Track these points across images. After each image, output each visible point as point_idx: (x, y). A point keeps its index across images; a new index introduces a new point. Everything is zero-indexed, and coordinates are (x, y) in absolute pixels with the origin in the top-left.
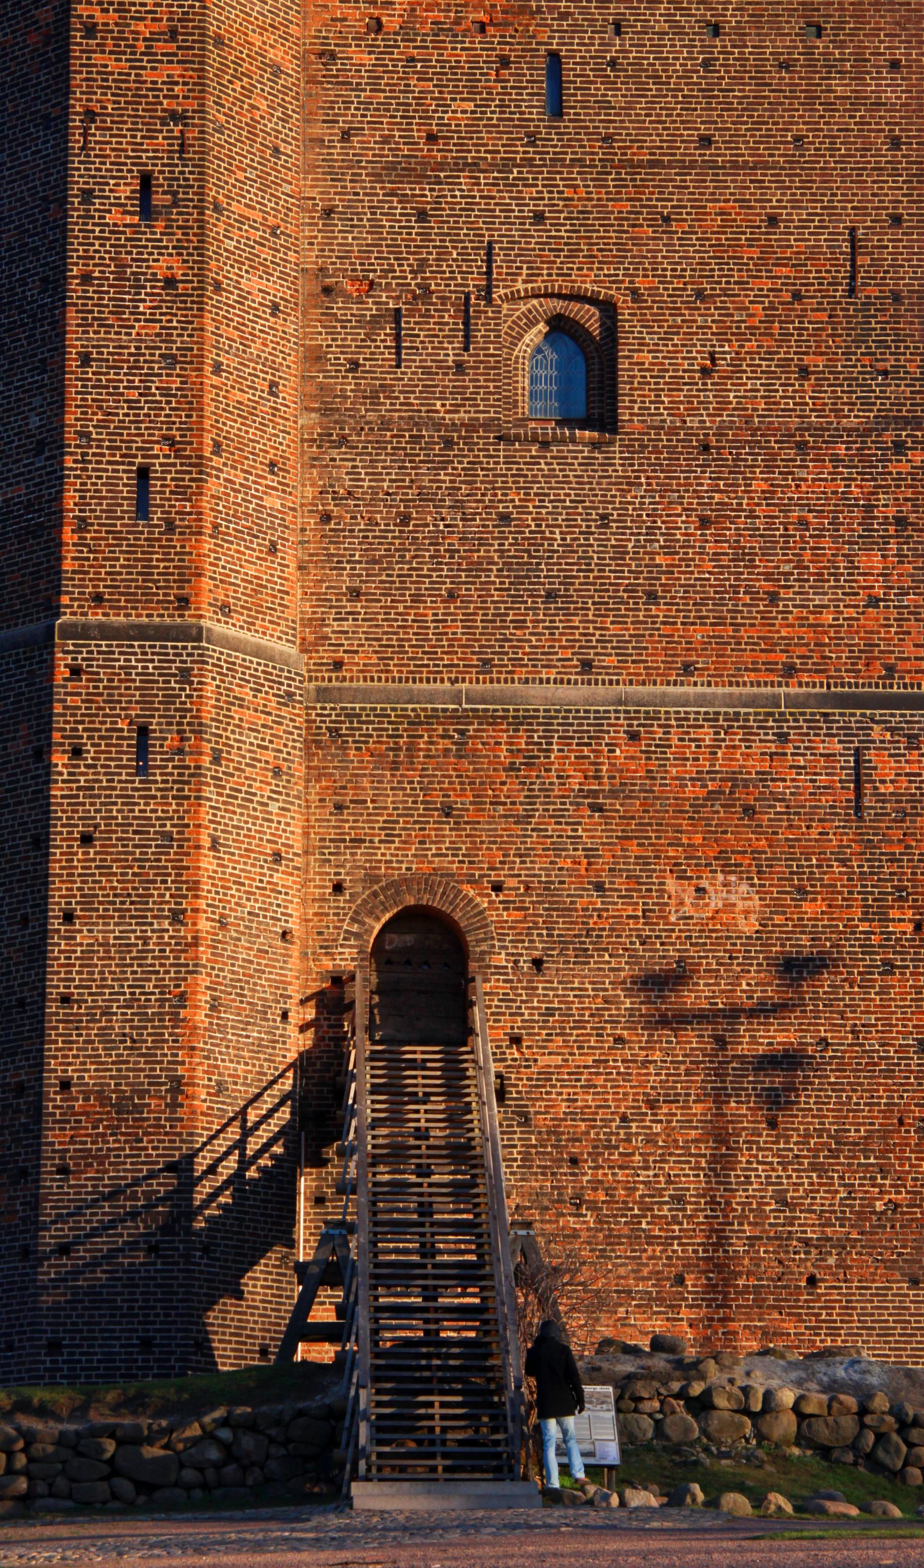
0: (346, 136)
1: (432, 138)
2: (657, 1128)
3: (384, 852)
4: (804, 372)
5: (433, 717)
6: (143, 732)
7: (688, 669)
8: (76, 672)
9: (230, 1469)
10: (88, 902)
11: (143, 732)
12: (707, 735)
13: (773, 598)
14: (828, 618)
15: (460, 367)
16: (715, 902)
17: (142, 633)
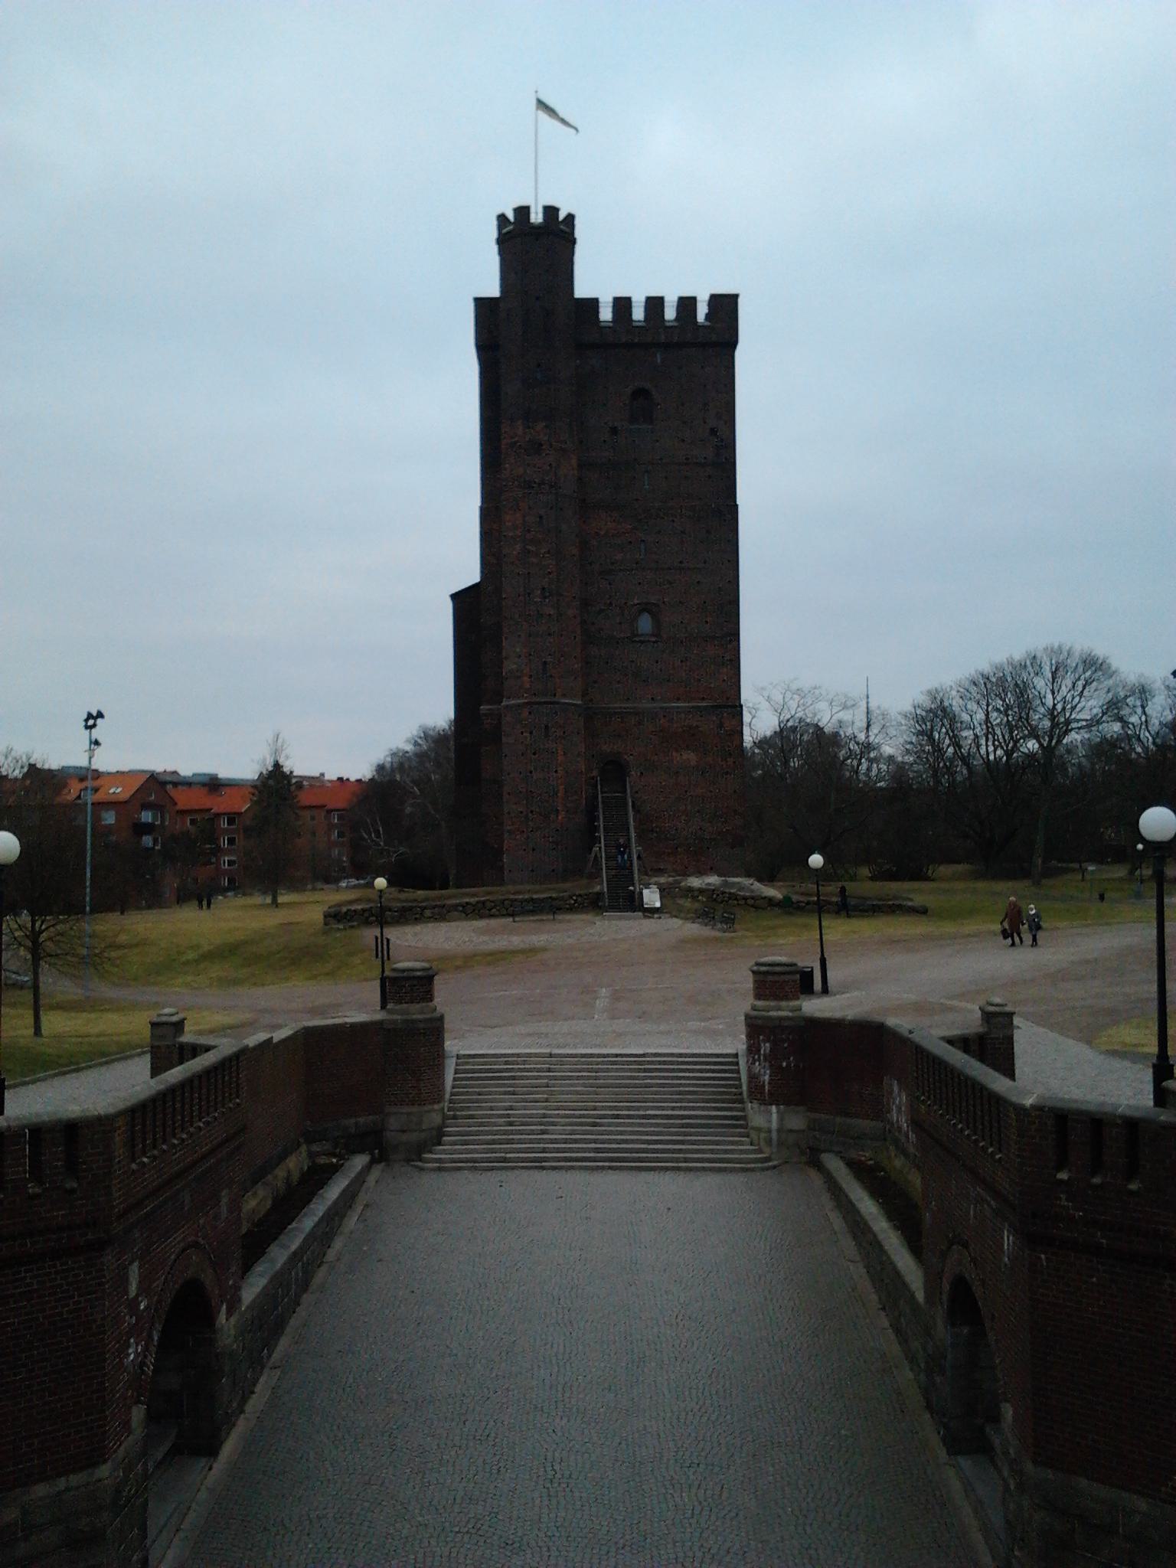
0: (591, 564)
1: (612, 564)
2: (671, 813)
3: (604, 747)
4: (707, 622)
5: (615, 713)
6: (547, 727)
7: (678, 699)
8: (530, 713)
9: (576, 905)
10: (535, 769)
11: (547, 727)
12: (683, 715)
13: (699, 680)
14: (712, 685)
15: (620, 623)
16: (685, 757)
17: (545, 703)
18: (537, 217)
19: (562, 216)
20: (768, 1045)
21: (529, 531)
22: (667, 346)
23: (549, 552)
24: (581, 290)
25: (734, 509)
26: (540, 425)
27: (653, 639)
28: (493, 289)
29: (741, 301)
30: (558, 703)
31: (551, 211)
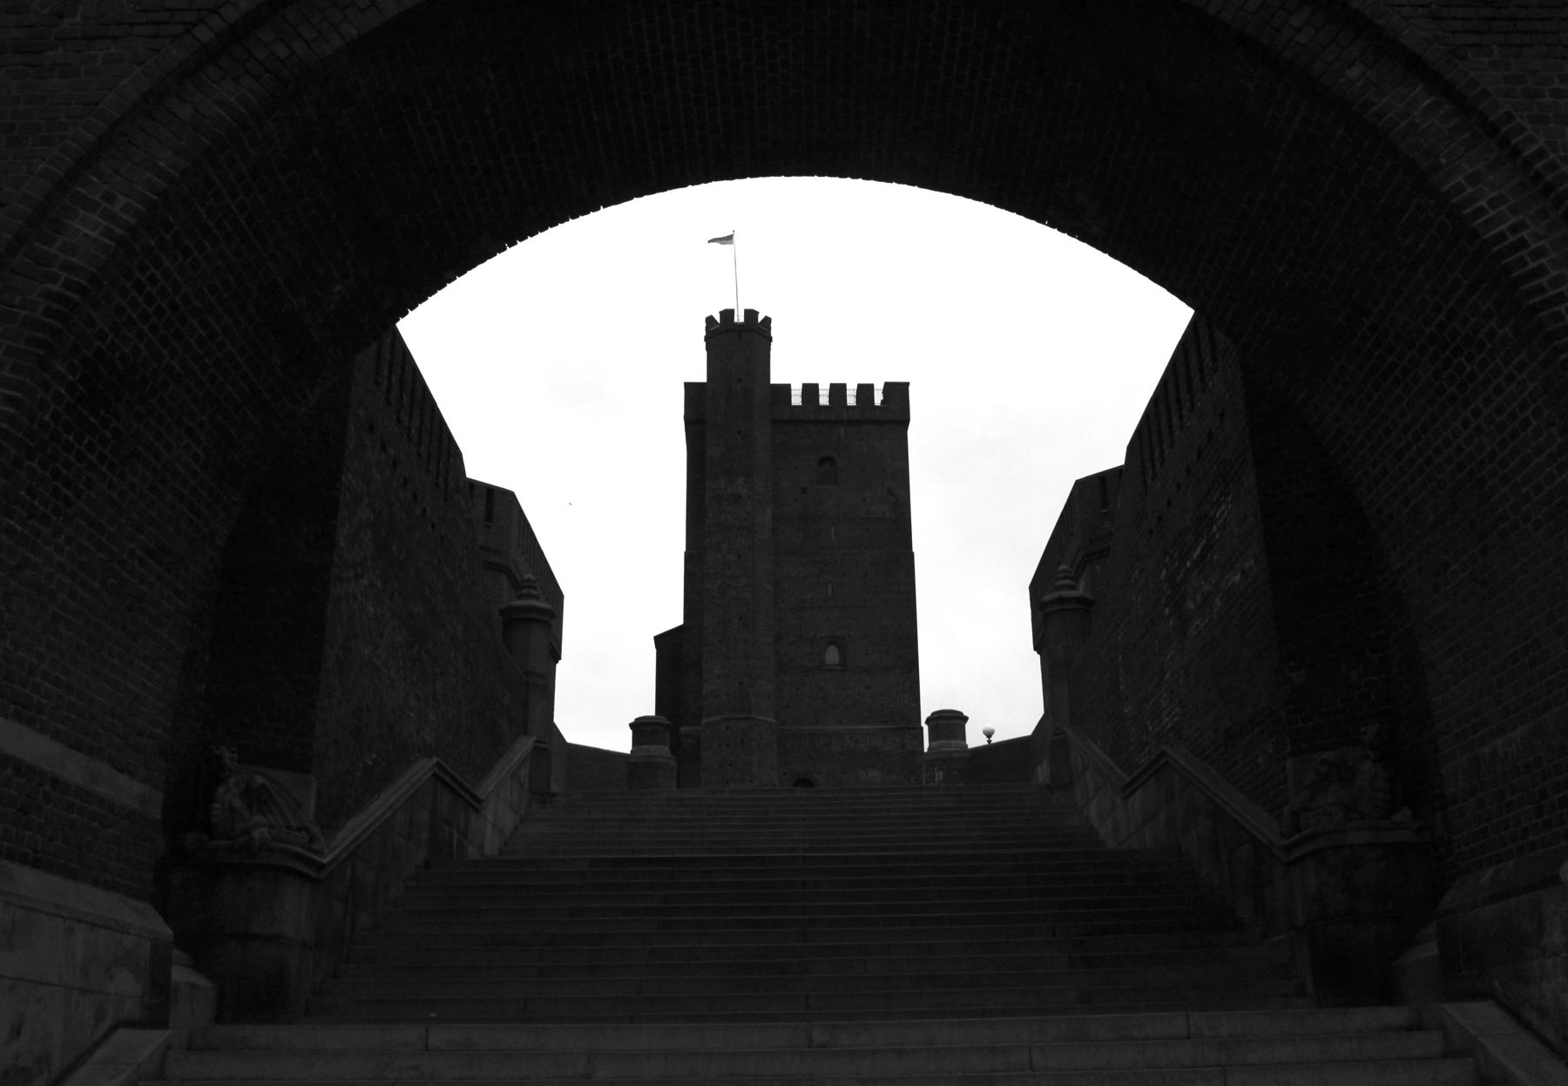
6: (742, 741)
8: (727, 728)
11: (742, 741)
12: (868, 737)
17: (744, 719)
18: (739, 318)
19: (760, 318)
20: (941, 773)
21: (729, 568)
22: (851, 422)
23: (746, 586)
24: (776, 378)
25: (911, 555)
26: (740, 480)
27: (840, 668)
28: (701, 376)
29: (910, 388)
30: (752, 719)
31: (751, 314)
